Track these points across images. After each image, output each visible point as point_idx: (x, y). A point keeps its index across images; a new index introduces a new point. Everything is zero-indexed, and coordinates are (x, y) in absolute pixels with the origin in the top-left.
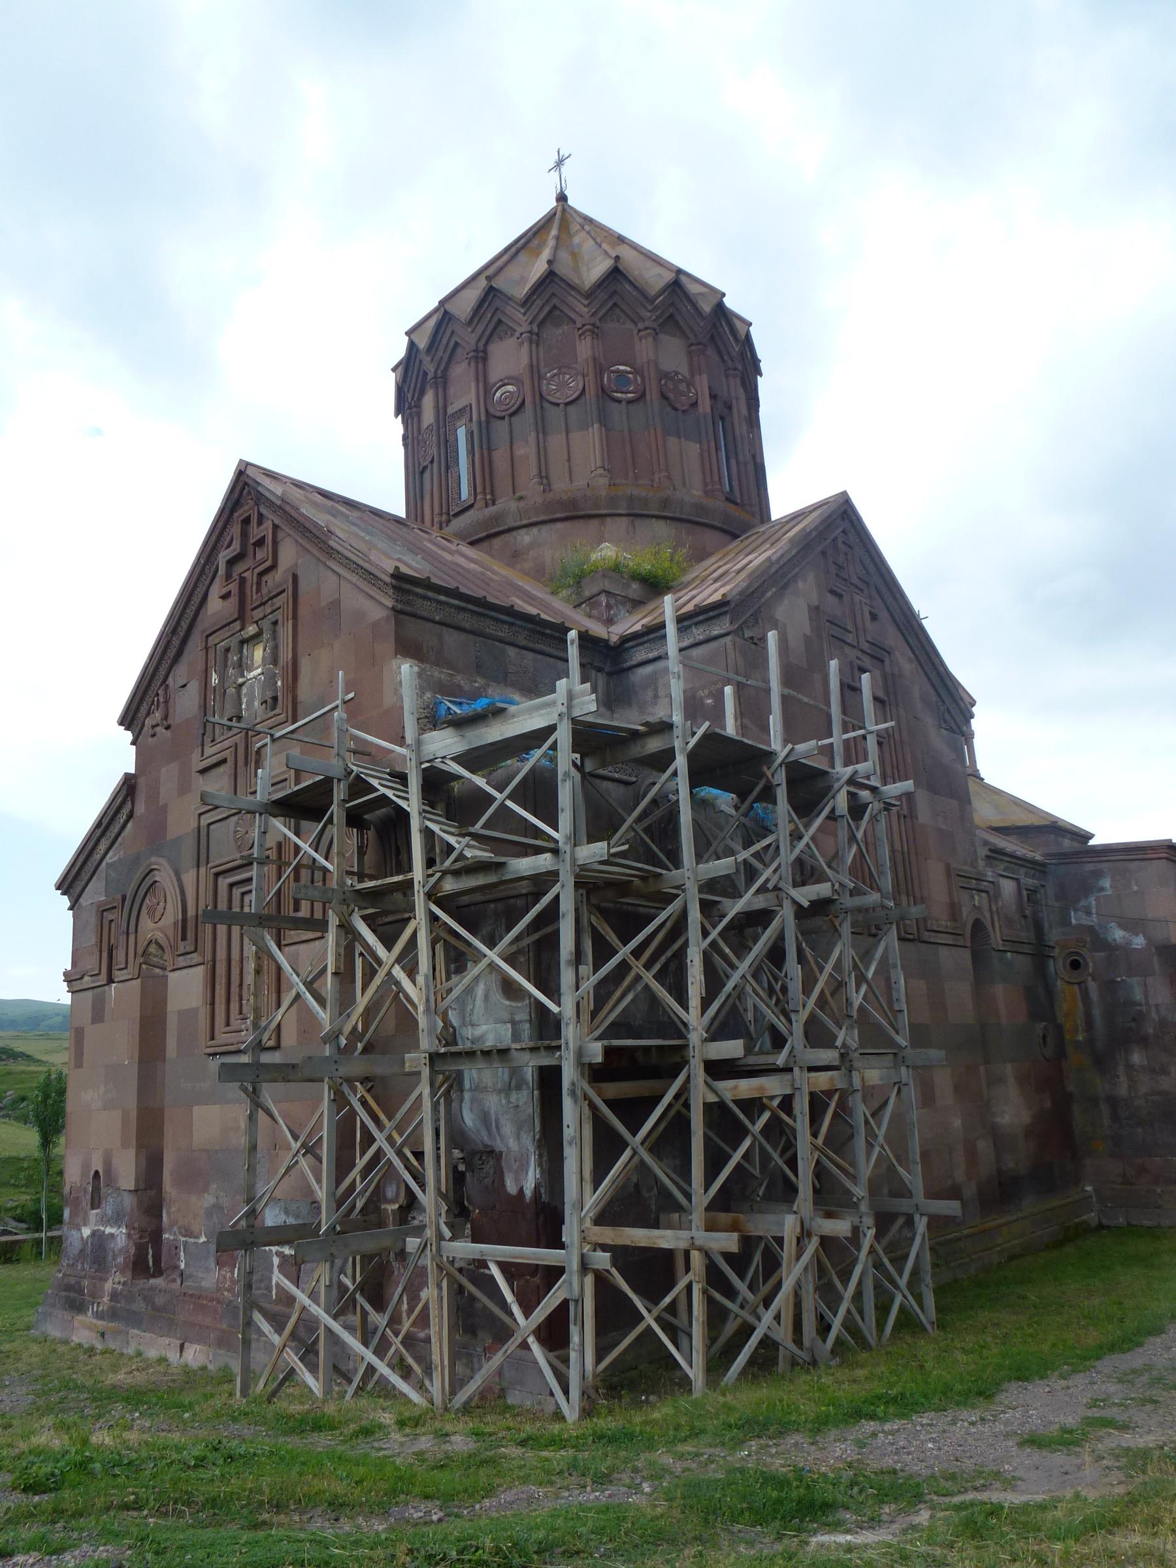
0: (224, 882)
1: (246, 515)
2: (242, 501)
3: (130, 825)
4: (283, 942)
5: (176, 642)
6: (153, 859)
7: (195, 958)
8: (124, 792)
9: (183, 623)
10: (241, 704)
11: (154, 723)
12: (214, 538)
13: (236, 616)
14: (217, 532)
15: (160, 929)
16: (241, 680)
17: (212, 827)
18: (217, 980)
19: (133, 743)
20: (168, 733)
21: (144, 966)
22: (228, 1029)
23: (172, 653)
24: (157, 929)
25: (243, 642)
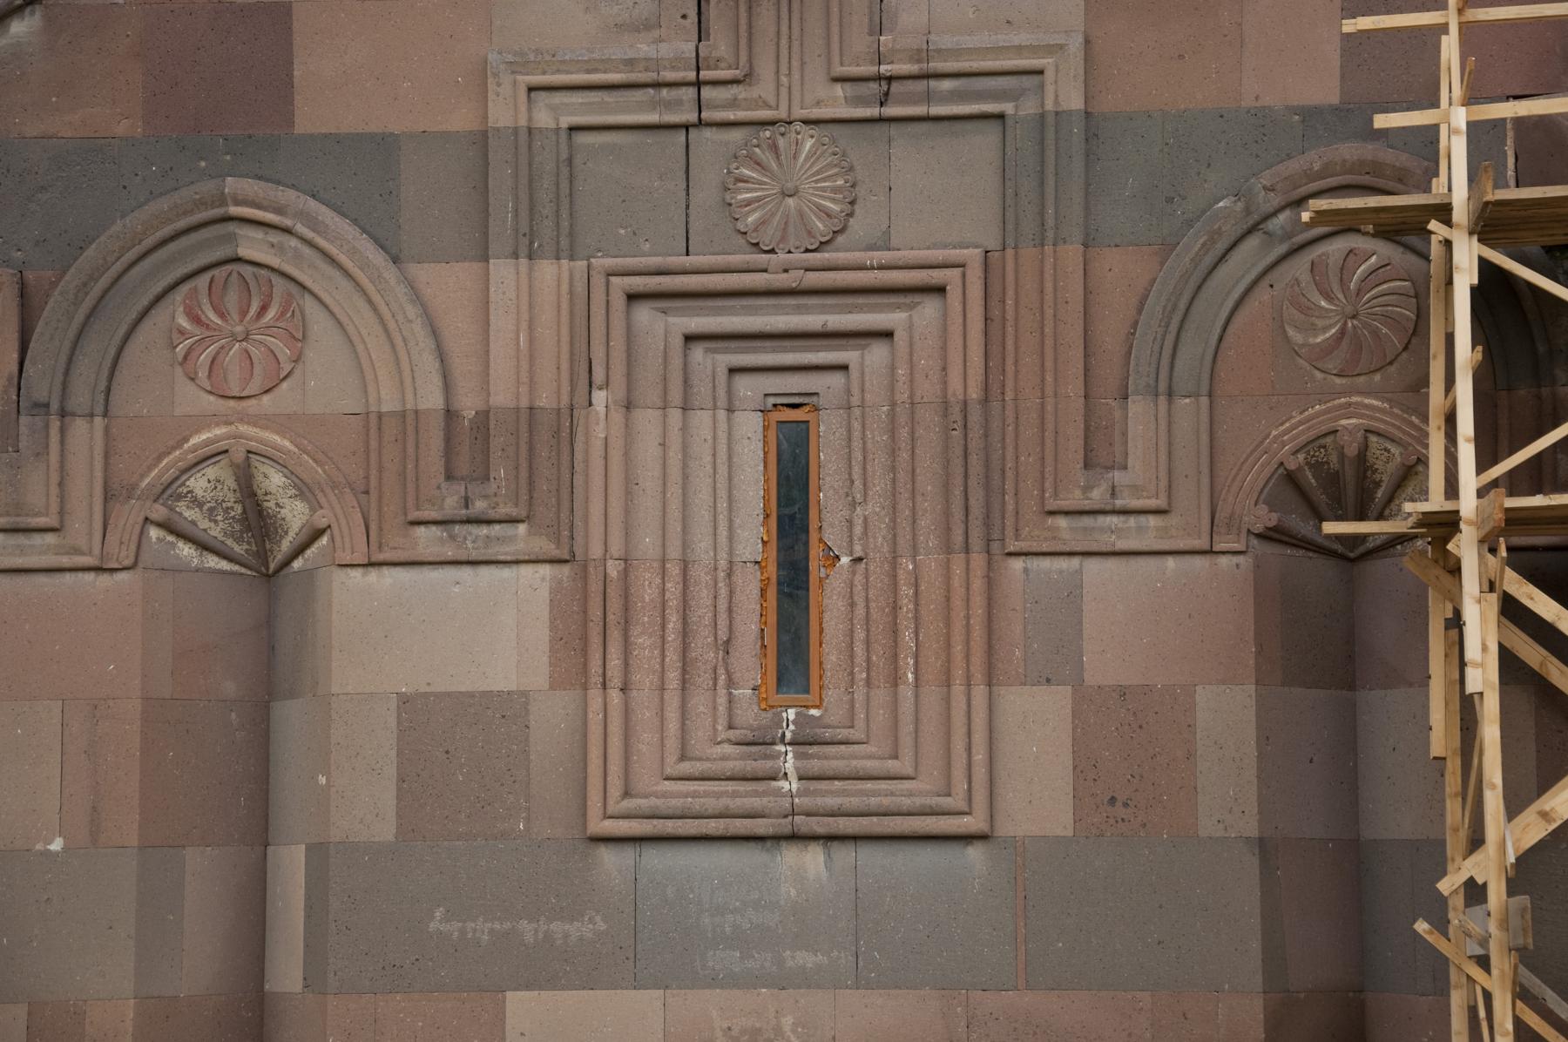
21: (154, 533)
24: (254, 421)
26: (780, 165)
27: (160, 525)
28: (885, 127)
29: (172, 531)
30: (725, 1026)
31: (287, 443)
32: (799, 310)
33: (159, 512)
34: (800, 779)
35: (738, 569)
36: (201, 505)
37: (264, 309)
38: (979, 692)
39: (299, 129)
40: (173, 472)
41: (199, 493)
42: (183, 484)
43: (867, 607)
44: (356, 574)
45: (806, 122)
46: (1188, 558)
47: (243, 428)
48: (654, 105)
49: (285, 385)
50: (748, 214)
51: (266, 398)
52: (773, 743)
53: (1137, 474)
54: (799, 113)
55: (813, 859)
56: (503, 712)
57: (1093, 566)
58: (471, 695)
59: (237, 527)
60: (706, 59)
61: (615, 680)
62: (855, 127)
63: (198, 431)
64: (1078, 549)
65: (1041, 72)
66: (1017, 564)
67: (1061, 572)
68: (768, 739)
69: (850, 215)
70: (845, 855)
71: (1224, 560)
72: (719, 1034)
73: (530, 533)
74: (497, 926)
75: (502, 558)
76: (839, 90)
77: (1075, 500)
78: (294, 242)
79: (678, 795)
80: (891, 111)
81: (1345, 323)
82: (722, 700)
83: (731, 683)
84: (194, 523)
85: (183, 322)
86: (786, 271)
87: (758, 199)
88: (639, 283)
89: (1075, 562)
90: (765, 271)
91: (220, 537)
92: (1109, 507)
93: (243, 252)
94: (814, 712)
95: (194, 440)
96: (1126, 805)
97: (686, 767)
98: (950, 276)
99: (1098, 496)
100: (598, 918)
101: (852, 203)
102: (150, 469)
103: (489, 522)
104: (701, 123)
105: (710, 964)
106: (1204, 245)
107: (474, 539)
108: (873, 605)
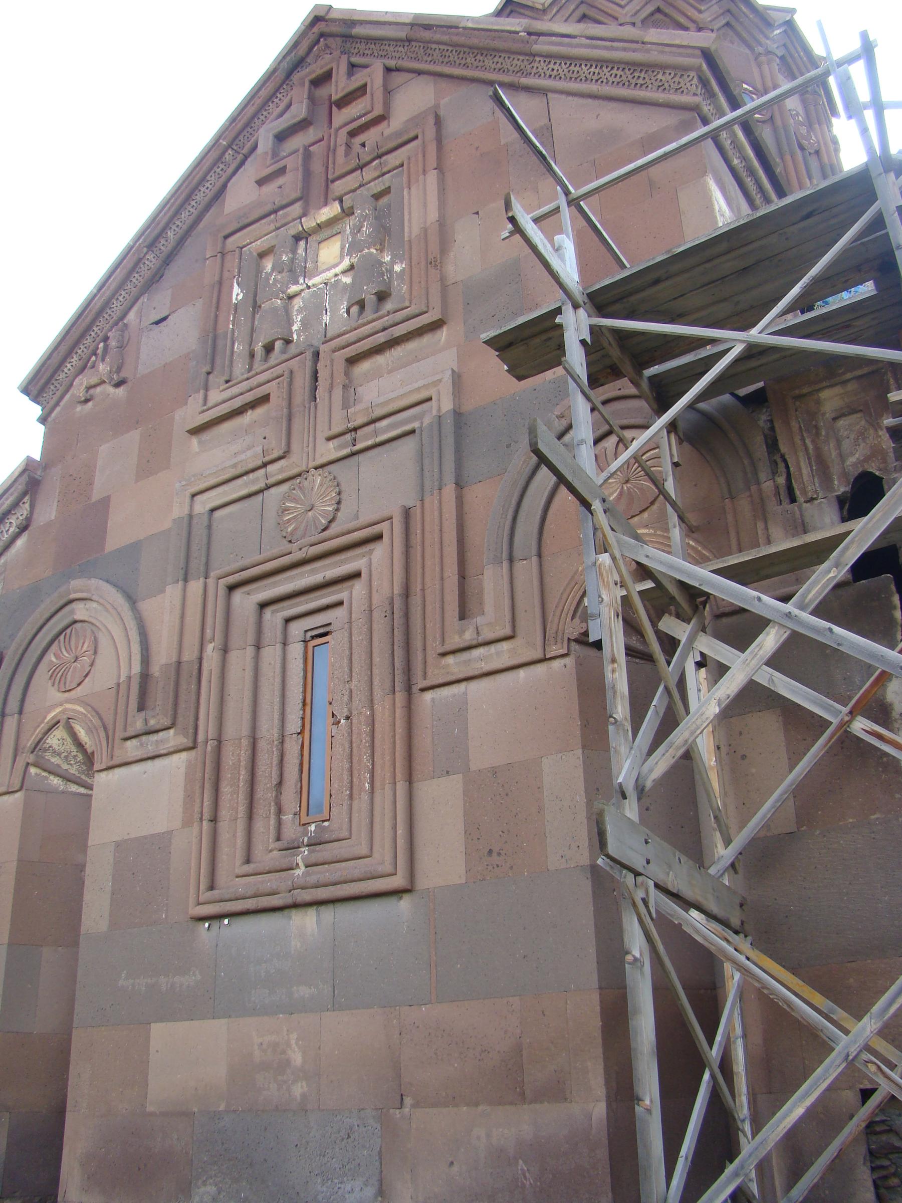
0: (245, 602)
1: (328, 67)
2: (308, 60)
3: (20, 543)
4: (420, 682)
5: (152, 261)
6: (75, 583)
7: (171, 739)
8: (20, 487)
9: (170, 234)
10: (290, 323)
11: (94, 380)
12: (251, 110)
13: (298, 194)
14: (258, 101)
15: (79, 701)
16: (293, 289)
17: (218, 514)
18: (227, 775)
19: (43, 420)
20: (121, 391)
21: (33, 770)
22: (247, 868)
23: (145, 272)
25: (297, 238)
26: (304, 496)
27: (36, 765)
28: (355, 458)
29: (45, 770)
30: (260, 1040)
31: (81, 709)
32: (313, 572)
33: (31, 758)
34: (306, 867)
35: (287, 739)
36: (59, 755)
37: (83, 643)
38: (401, 787)
39: (106, 551)
40: (40, 736)
41: (56, 747)
42: (45, 743)
43: (351, 747)
44: (103, 775)
45: (316, 468)
46: (532, 667)
47: (68, 706)
48: (246, 484)
49: (87, 679)
50: (286, 528)
51: (79, 688)
52: (299, 847)
53: (490, 618)
54: (312, 464)
55: (307, 922)
56: (159, 843)
57: (473, 686)
58: (145, 837)
59: (85, 768)
60: (267, 450)
61: (206, 816)
62: (341, 463)
63: (49, 712)
64: (461, 676)
65: (430, 399)
66: (428, 696)
67: (454, 696)
68: (296, 844)
69: (337, 510)
70: (328, 913)
71: (557, 664)
72: (256, 1047)
73: (175, 734)
74: (149, 981)
75: (162, 752)
76: (331, 444)
77: (455, 641)
78: (94, 605)
79: (242, 886)
80: (359, 446)
81: (622, 488)
82: (273, 821)
83: (279, 811)
84: (58, 766)
85: (54, 659)
86: (300, 549)
87: (294, 518)
88: (231, 580)
89: (463, 686)
90: (290, 553)
91: (76, 773)
92: (474, 642)
93: (78, 617)
94: (326, 824)
95: (49, 718)
96: (499, 854)
97: (247, 868)
98: (384, 527)
99: (469, 636)
100: (197, 972)
101: (339, 503)
102: (32, 736)
103: (157, 731)
104: (268, 487)
105: (253, 999)
106: (524, 462)
107: (151, 743)
108: (354, 745)
